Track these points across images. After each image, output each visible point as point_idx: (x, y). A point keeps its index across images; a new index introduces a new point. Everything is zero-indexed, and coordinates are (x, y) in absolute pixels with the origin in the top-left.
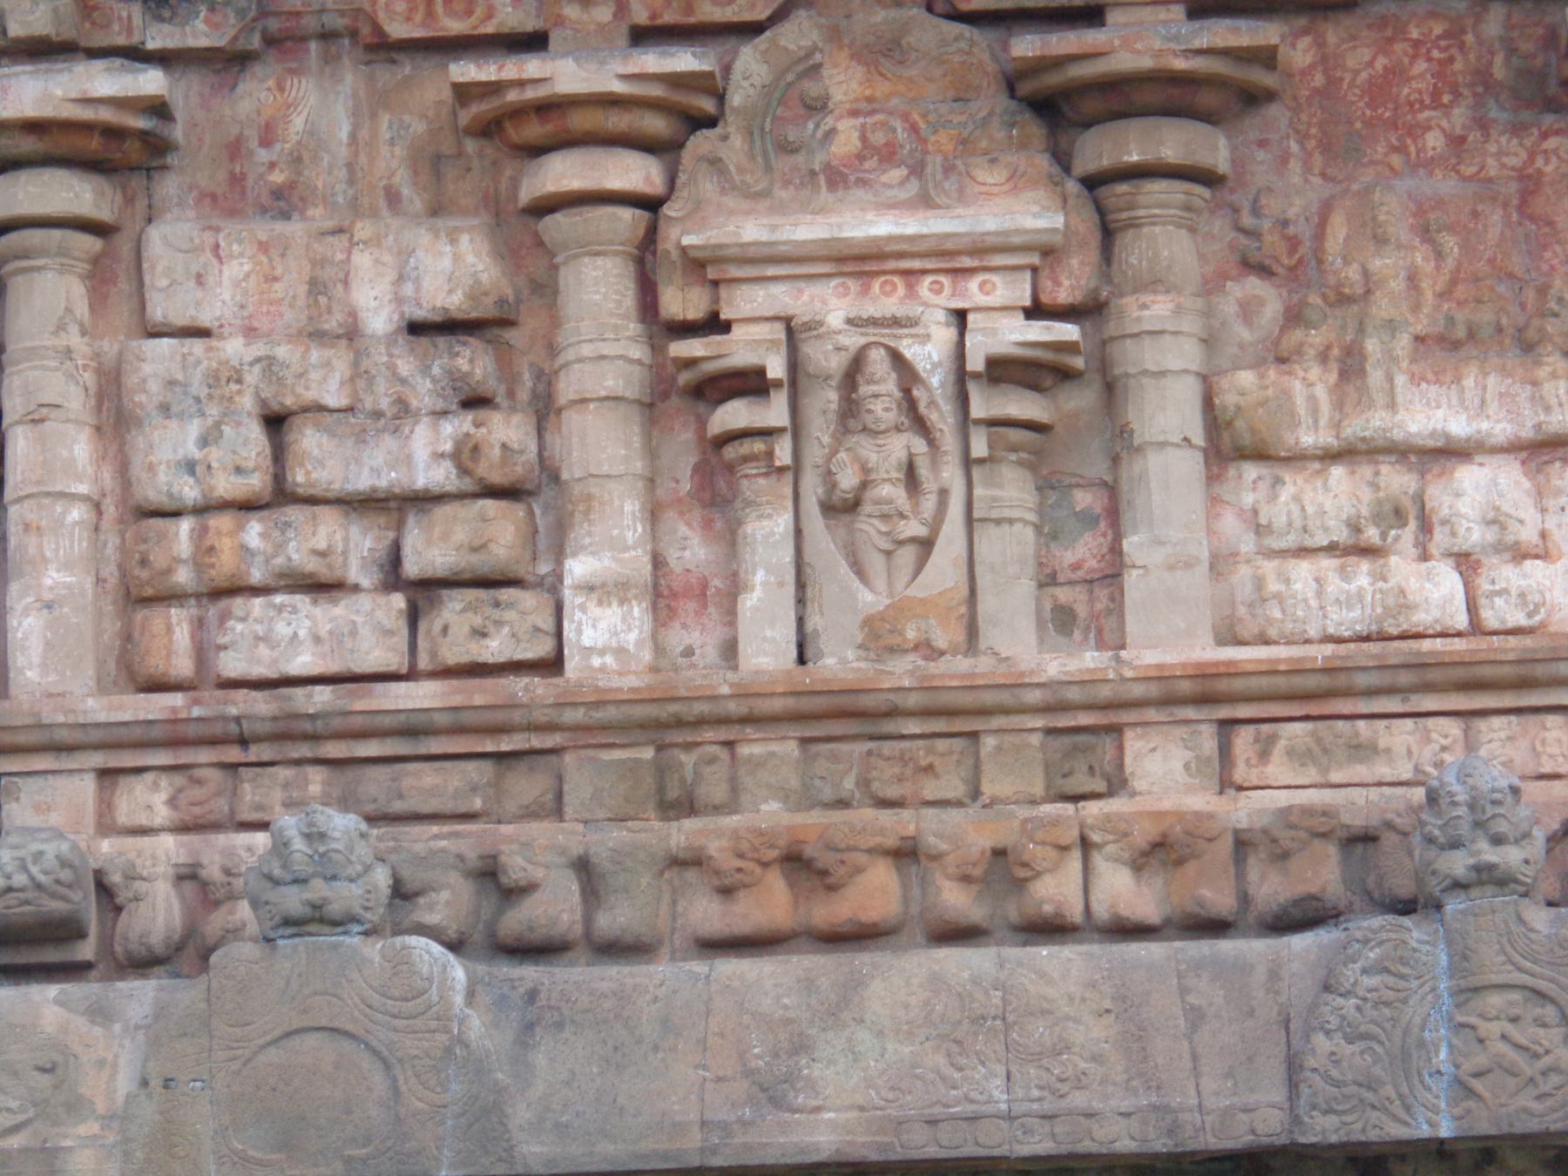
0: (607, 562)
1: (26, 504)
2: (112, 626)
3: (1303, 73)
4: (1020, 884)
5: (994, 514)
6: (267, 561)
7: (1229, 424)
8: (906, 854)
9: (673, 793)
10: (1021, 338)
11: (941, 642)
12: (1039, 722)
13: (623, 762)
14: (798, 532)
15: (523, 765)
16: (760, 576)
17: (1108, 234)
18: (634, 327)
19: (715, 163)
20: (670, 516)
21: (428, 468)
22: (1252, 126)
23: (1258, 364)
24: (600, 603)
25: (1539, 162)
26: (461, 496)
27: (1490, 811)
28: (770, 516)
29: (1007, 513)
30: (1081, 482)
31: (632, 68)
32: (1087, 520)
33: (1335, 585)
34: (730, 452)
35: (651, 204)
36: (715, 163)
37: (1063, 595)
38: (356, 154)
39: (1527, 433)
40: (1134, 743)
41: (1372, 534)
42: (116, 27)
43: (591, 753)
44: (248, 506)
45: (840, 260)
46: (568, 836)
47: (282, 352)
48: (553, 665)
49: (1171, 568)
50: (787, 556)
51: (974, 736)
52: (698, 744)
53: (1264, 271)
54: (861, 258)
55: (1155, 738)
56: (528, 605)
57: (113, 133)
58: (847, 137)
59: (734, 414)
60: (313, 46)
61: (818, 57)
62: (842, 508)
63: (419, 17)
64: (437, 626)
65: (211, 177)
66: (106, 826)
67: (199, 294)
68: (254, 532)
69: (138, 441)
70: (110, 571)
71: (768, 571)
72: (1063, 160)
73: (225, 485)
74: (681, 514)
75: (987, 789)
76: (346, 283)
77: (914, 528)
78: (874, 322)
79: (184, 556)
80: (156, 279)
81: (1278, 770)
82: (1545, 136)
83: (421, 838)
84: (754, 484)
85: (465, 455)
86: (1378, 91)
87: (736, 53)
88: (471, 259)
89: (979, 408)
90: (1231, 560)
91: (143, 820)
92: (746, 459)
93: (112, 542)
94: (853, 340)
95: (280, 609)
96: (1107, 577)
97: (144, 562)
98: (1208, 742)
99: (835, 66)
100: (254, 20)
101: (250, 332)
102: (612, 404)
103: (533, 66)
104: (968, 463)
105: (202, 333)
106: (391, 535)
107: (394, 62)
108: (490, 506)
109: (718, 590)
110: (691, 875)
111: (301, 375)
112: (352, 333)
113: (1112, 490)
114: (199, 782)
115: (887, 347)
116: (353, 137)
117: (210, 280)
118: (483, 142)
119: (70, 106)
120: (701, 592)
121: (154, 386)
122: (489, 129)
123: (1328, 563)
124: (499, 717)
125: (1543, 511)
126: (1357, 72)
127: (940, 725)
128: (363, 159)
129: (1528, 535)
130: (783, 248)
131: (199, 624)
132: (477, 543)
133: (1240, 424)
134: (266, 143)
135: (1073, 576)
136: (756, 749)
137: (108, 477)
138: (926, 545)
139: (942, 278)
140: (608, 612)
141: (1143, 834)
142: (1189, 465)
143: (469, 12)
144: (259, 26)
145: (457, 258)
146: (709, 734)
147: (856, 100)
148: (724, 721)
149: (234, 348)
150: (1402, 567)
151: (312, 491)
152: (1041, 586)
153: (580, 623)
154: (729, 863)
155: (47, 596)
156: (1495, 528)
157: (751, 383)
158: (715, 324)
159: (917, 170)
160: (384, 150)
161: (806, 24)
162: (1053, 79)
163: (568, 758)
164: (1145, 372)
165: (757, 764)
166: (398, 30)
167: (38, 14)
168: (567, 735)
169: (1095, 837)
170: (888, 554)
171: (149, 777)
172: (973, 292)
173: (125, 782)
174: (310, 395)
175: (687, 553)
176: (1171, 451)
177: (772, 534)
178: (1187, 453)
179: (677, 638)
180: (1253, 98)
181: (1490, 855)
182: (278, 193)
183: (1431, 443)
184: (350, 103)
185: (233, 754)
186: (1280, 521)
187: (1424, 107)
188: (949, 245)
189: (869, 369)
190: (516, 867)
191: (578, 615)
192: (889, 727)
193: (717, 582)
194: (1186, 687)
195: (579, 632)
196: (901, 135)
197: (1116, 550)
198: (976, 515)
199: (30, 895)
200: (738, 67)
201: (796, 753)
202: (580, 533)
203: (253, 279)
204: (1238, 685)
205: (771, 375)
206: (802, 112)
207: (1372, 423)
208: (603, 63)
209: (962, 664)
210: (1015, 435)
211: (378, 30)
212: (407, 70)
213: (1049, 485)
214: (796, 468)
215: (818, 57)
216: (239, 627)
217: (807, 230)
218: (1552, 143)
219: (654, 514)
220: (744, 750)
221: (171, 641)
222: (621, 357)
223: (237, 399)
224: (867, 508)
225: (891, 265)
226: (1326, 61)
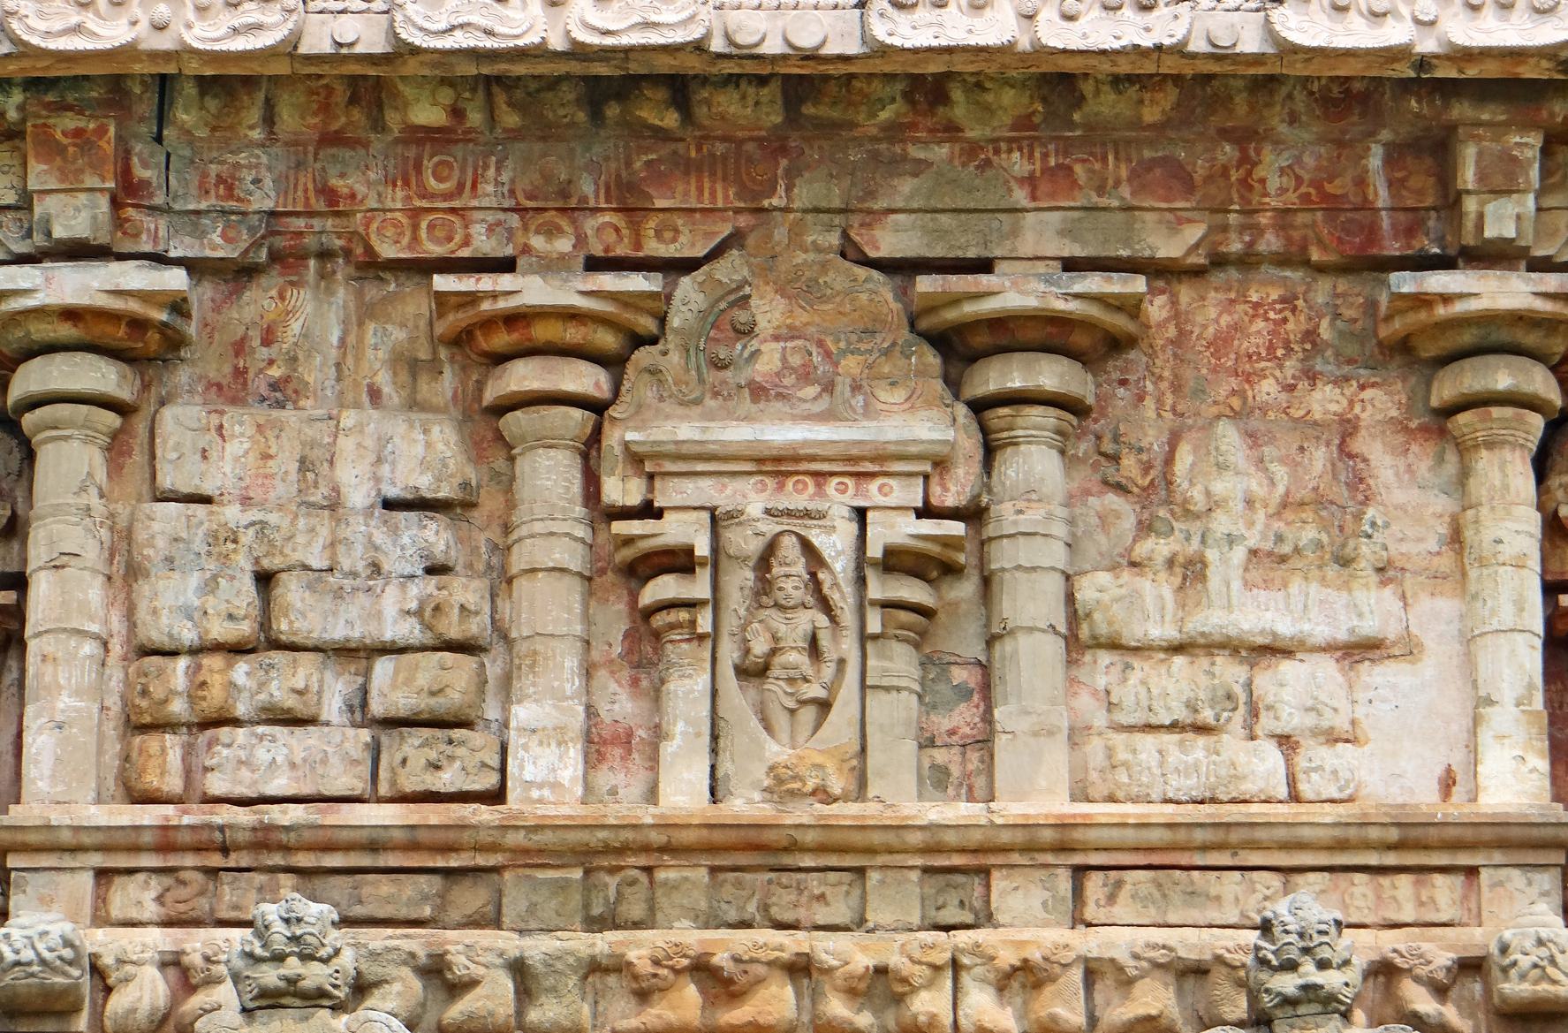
0: (548, 709)
1: (45, 638)
2: (114, 748)
3: (1159, 325)
4: (899, 1000)
5: (885, 682)
6: (252, 696)
7: (1088, 615)
8: (800, 969)
9: (596, 911)
10: (915, 532)
11: (837, 790)
12: (918, 861)
13: (557, 880)
14: (714, 694)
15: (468, 882)
16: (680, 727)
17: (990, 451)
18: (579, 510)
19: (654, 372)
20: (602, 675)
21: (395, 622)
22: (1114, 368)
23: (1113, 568)
24: (541, 743)
25: (1357, 409)
26: (423, 648)
27: (1317, 939)
28: (690, 676)
29: (895, 682)
31: (589, 287)
32: (964, 693)
33: (1174, 757)
34: (659, 620)
35: (597, 407)
36: (654, 372)
37: (940, 756)
38: (345, 354)
39: (1342, 636)
40: (999, 882)
41: (1207, 715)
42: (144, 237)
43: (528, 871)
44: (237, 650)
45: (760, 460)
46: (507, 942)
47: (273, 518)
48: (496, 796)
49: (1035, 734)
51: (860, 872)
52: (621, 868)
53: (1120, 488)
54: (778, 460)
55: (1018, 878)
56: (479, 740)
57: (138, 325)
58: (769, 360)
59: (665, 587)
60: (312, 263)
61: (747, 290)
62: (753, 672)
63: (405, 240)
64: (398, 757)
65: (219, 370)
66: (101, 919)
67: (203, 466)
68: (241, 670)
69: (143, 588)
70: (114, 702)
71: (687, 723)
72: (954, 384)
73: (220, 630)
74: (612, 673)
75: (872, 918)
76: (331, 463)
77: (815, 691)
78: (789, 513)
79: (180, 689)
80: (165, 452)
81: (1122, 911)
82: (1362, 388)
83: (377, 938)
84: (679, 650)
85: (428, 613)
86: (1220, 343)
87: (676, 284)
88: (440, 446)
89: (875, 590)
91: (134, 914)
93: (115, 676)
94: (770, 528)
95: (261, 738)
97: (145, 693)
98: (1064, 883)
99: (762, 298)
100: (263, 237)
101: (246, 501)
102: (557, 574)
103: (505, 281)
104: (864, 638)
105: (206, 500)
106: (360, 680)
108: (447, 656)
109: (642, 739)
110: (612, 980)
111: (290, 538)
112: (334, 505)
113: (985, 668)
114: (183, 883)
115: (797, 534)
116: (343, 342)
117: (213, 455)
118: (455, 350)
119: (105, 296)
120: (625, 740)
121: (161, 542)
122: (460, 340)
123: (1171, 739)
124: (451, 836)
125: (1354, 702)
126: (1205, 327)
127: (833, 861)
128: (350, 361)
129: (1341, 723)
131: (188, 751)
132: (436, 688)
133: (1097, 616)
134: (267, 342)
137: (117, 624)
138: (824, 706)
140: (548, 751)
141: (1008, 958)
142: (1053, 648)
143: (450, 239)
144: (267, 243)
145: (428, 445)
146: (632, 860)
147: (778, 327)
148: (646, 849)
149: (232, 513)
150: (1232, 743)
151: (294, 639)
152: (921, 747)
154: (644, 967)
155: (60, 717)
156: (1313, 714)
157: (680, 561)
158: (648, 511)
159: (829, 387)
160: (370, 353)
161: (737, 262)
162: (951, 315)
163: (507, 875)
164: (1019, 567)
165: (673, 887)
166: (387, 251)
167: (80, 220)
168: (508, 855)
169: (966, 960)
170: (792, 712)
171: (141, 877)
172: (873, 493)
173: (119, 881)
174: (296, 557)
175: (616, 707)
176: (1038, 635)
178: (1050, 638)
179: (605, 778)
180: (1117, 344)
181: (1318, 978)
182: (275, 386)
183: (1260, 640)
184: (341, 312)
185: (216, 860)
186: (1129, 701)
187: (1260, 359)
188: (855, 452)
189: (781, 553)
190: (461, 965)
191: (521, 753)
192: (787, 860)
193: (641, 733)
194: (1048, 836)
195: (521, 768)
196: (816, 359)
197: (988, 718)
198: (869, 682)
199: (36, 968)
200: (678, 294)
201: (706, 879)
202: (524, 684)
203: (251, 457)
205: (698, 553)
206: (732, 334)
207: (1210, 620)
208: (566, 281)
209: (848, 811)
210: (904, 616)
211: (369, 250)
212: (392, 287)
213: (933, 664)
214: (715, 636)
215: (747, 290)
216: (225, 752)
217: (736, 433)
218: (1368, 394)
219: (588, 671)
220: (661, 875)
221: (165, 761)
222: (567, 534)
223: (232, 556)
224: (775, 672)
225: (804, 466)
226: (1177, 316)
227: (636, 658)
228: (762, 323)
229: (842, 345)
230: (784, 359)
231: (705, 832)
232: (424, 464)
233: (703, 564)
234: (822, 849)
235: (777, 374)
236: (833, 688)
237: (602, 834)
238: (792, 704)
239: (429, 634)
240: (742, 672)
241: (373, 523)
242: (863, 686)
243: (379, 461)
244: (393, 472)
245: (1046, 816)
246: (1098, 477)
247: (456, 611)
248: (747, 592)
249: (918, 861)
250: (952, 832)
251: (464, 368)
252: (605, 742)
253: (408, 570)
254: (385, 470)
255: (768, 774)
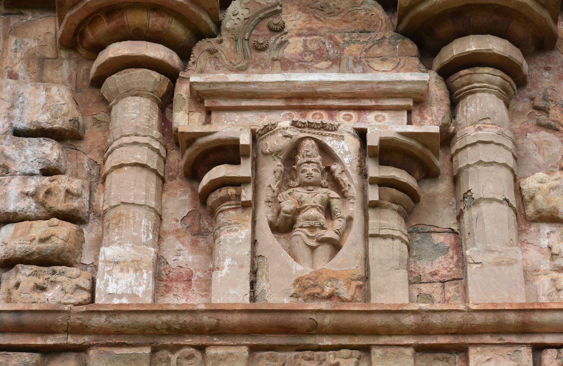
0: (128, 249)
5: (383, 232)
7: (532, 198)
10: (402, 130)
11: (346, 295)
12: (412, 341)
13: (130, 355)
14: (254, 242)
16: (228, 261)
18: (156, 133)
19: (212, 52)
20: (170, 239)
21: (17, 200)
24: (122, 270)
26: (37, 218)
28: (236, 231)
29: (390, 232)
30: (437, 230)
32: (441, 250)
34: (213, 198)
43: (108, 349)
45: (288, 98)
49: (498, 264)
50: (246, 250)
51: (366, 349)
54: (301, 97)
55: (489, 353)
64: (13, 282)
71: (233, 259)
74: (178, 237)
77: (329, 234)
78: (310, 125)
88: (57, 98)
90: (535, 273)
92: (223, 200)
94: (297, 134)
96: (454, 279)
102: (139, 169)
107: (23, 14)
108: (55, 221)
115: (316, 140)
118: (72, 52)
124: (49, 318)
127: (345, 341)
130: (253, 86)
132: (44, 236)
133: (539, 197)
135: (432, 279)
136: (220, 351)
139: (351, 113)
140: (127, 275)
145: (48, 97)
146: (189, 341)
147: (301, 29)
148: (199, 331)
152: (410, 283)
153: (107, 280)
160: (11, 54)
163: (91, 352)
164: (480, 162)
168: (93, 337)
170: (313, 249)
175: (181, 258)
176: (496, 204)
177: (237, 239)
178: (505, 207)
188: (357, 89)
189: (303, 151)
191: (106, 276)
193: (199, 274)
194: (512, 318)
195: (106, 285)
196: (328, 46)
198: (370, 232)
201: (247, 354)
204: (547, 317)
205: (242, 142)
206: (268, 32)
210: (394, 192)
215: (279, 8)
220: (211, 351)
222: (147, 144)
224: (300, 223)
225: (320, 103)
227: (196, 229)
228: (289, 26)
229: (347, 39)
230: (305, 46)
231: (245, 317)
232: (46, 108)
233: (246, 156)
234: (337, 331)
235: (301, 54)
236: (342, 234)
237: (166, 318)
238: (313, 243)
239: (42, 209)
240: (276, 229)
241: (6, 143)
242: (367, 236)
243: (12, 107)
244: (22, 113)
245: (511, 304)
246: (534, 122)
247: (63, 193)
248: (278, 174)
249: (412, 341)
250: (437, 315)
251: (78, 62)
252: (171, 280)
253: (29, 170)
254: (16, 112)
255: (294, 285)
